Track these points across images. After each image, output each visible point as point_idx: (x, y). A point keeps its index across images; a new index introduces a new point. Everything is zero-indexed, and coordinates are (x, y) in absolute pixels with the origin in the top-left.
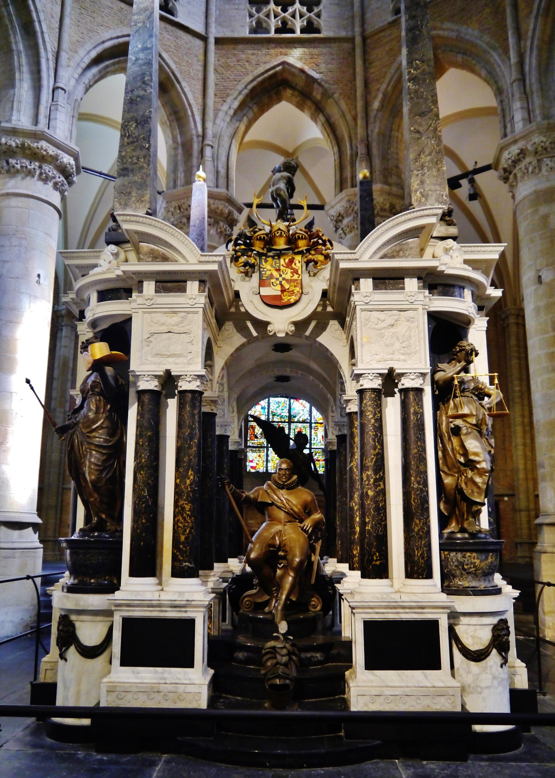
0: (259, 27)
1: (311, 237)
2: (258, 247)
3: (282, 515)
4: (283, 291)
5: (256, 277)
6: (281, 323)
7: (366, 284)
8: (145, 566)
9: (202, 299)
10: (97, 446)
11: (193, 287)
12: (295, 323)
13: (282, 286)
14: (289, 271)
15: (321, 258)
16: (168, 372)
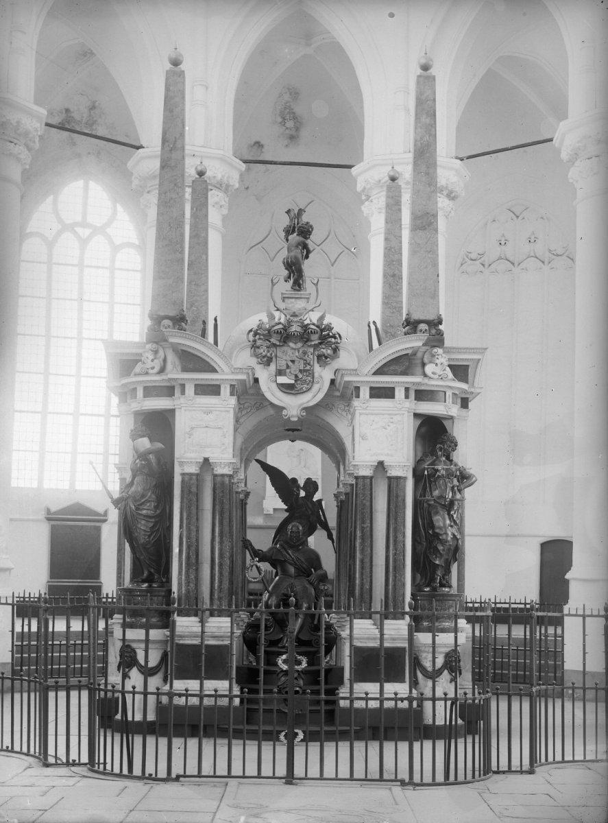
1: (322, 330)
3: (292, 570)
4: (296, 381)
5: (273, 367)
6: (293, 406)
8: (192, 607)
9: (233, 401)
10: (144, 516)
12: (305, 409)
13: (296, 376)
14: (302, 362)
15: (330, 352)
16: (206, 460)
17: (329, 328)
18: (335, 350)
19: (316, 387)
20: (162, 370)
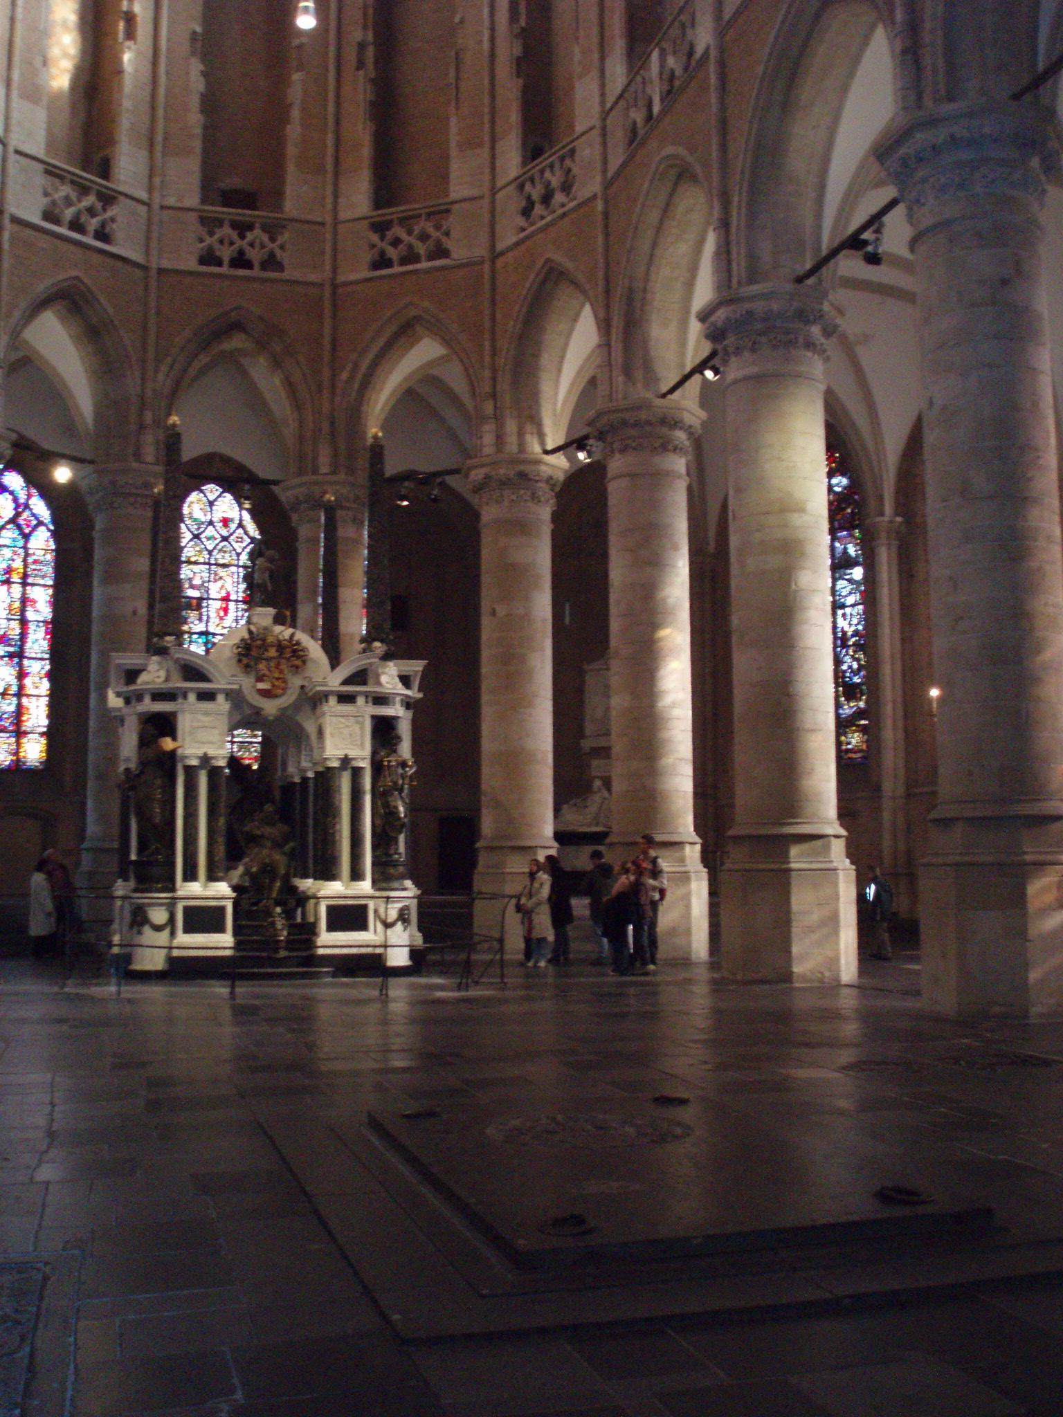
0: (209, 258)
2: (254, 653)
3: (269, 844)
4: (273, 686)
7: (333, 701)
8: (190, 875)
11: (221, 698)
17: (298, 643)
18: (304, 662)
19: (289, 692)
20: (167, 679)
